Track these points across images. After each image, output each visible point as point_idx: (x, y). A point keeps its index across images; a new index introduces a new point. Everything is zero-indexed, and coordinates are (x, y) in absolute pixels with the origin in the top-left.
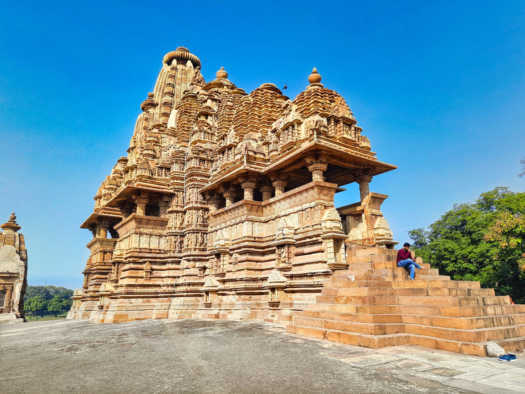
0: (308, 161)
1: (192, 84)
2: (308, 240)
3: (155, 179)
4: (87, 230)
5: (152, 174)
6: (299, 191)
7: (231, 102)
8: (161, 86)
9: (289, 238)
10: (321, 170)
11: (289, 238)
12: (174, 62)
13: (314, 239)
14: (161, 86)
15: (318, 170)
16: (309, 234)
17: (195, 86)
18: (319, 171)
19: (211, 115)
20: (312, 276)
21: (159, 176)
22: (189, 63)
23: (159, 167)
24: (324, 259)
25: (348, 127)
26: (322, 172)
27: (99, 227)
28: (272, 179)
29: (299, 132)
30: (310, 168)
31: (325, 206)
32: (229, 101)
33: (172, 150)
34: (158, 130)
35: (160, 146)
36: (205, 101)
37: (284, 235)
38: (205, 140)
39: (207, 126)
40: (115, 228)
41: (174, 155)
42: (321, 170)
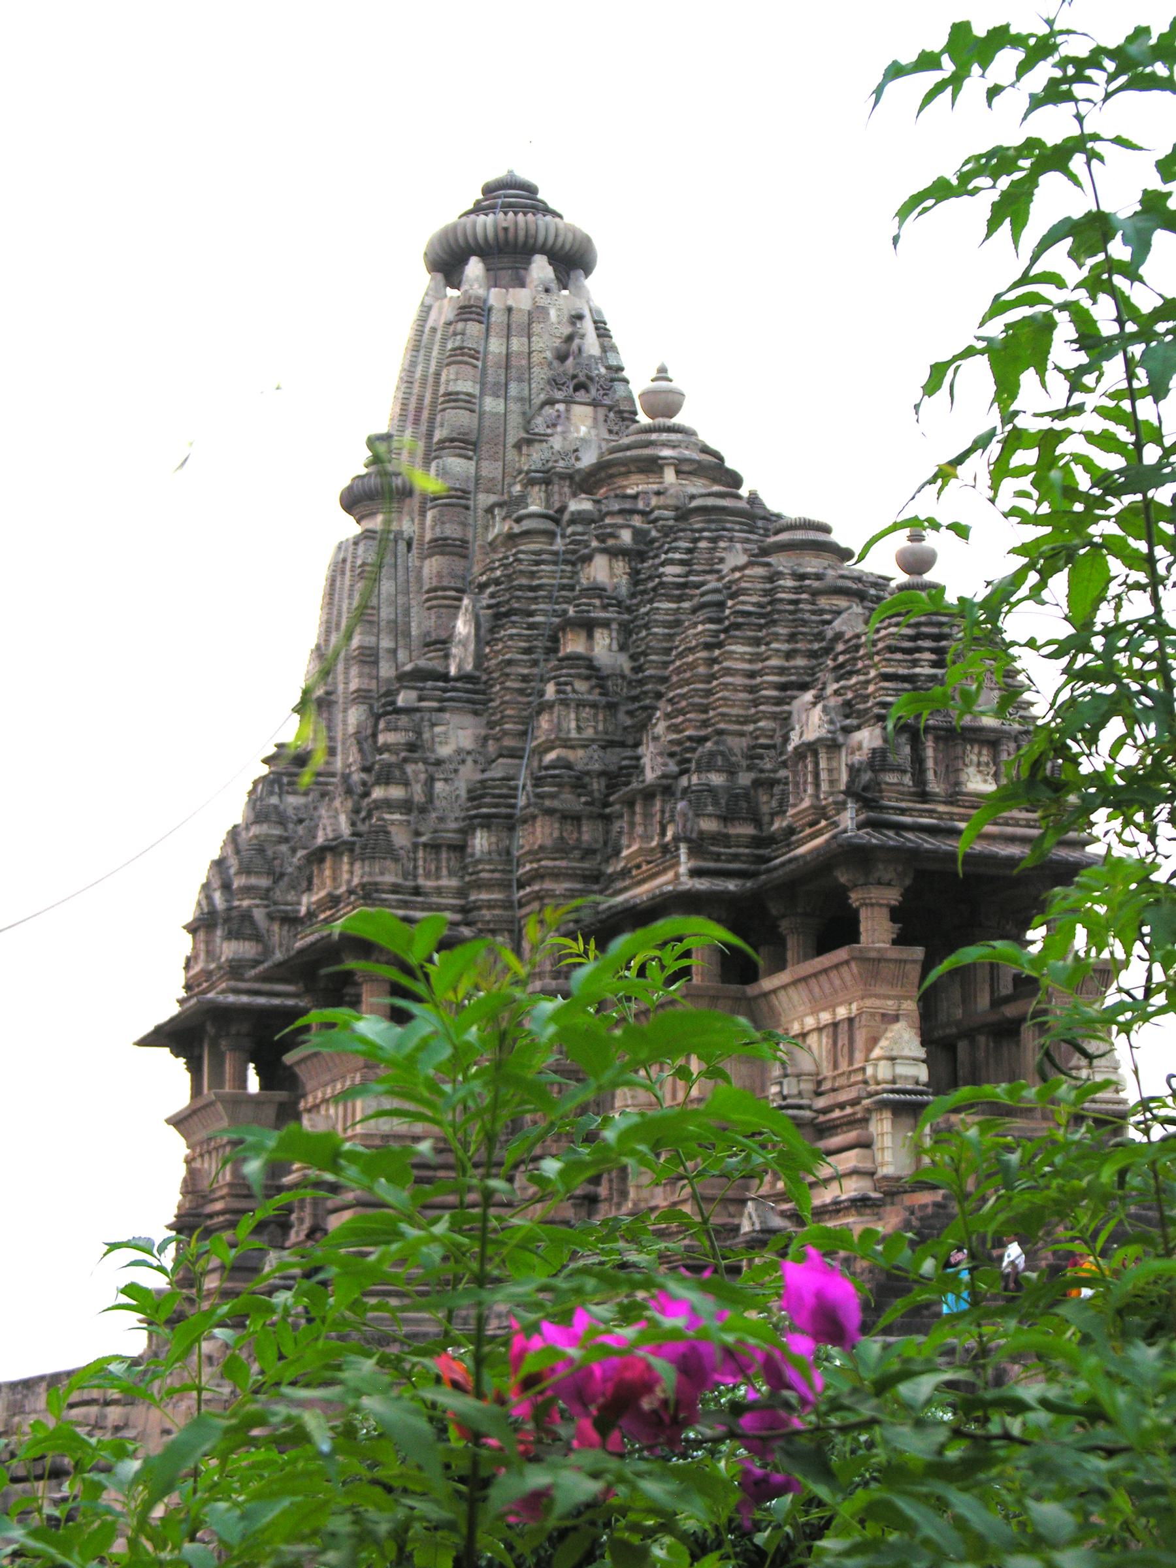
0: (843, 878)
1: (551, 402)
2: (837, 1113)
3: (417, 891)
4: (163, 1054)
5: (405, 875)
6: (819, 968)
7: (682, 562)
8: (421, 399)
9: (800, 1107)
10: (881, 905)
11: (800, 1107)
12: (474, 268)
13: (849, 1110)
14: (421, 399)
15: (872, 905)
16: (843, 1097)
17: (561, 407)
18: (877, 909)
19: (606, 624)
20: (838, 1211)
21: (427, 875)
22: (541, 269)
23: (425, 845)
24: (867, 1165)
25: (985, 752)
26: (885, 912)
27: (214, 1045)
28: (774, 912)
29: (836, 776)
30: (854, 898)
31: (883, 1015)
32: (671, 562)
33: (468, 774)
34: (413, 695)
35: (425, 761)
36: (588, 559)
37: (785, 1098)
38: (584, 736)
39: (588, 678)
40: (289, 1058)
41: (476, 795)
42: (881, 905)
